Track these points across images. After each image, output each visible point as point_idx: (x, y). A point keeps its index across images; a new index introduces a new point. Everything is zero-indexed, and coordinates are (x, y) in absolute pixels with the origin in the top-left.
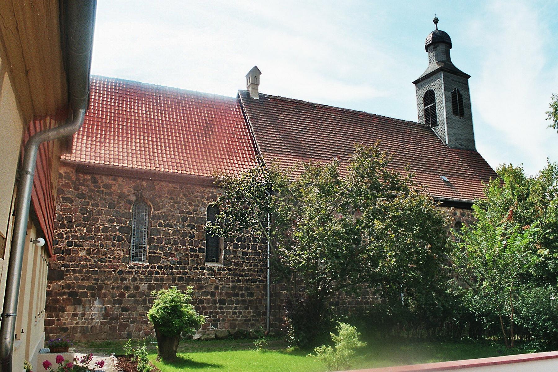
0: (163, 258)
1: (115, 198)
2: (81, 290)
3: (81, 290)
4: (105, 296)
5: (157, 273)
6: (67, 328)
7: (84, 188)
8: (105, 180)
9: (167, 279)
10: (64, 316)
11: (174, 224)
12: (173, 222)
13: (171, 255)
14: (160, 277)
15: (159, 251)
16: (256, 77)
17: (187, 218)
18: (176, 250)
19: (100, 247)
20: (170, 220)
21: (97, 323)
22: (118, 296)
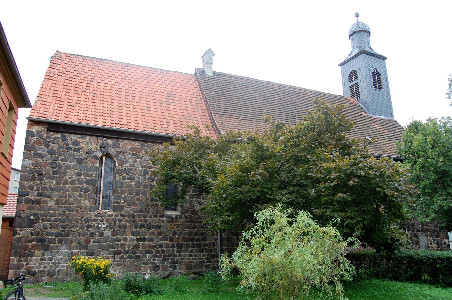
0: (126, 207)
1: (83, 154)
2: (49, 237)
3: (49, 237)
4: (72, 242)
5: (120, 221)
6: (35, 272)
7: (54, 145)
8: (73, 138)
9: (129, 226)
10: (32, 260)
11: (137, 177)
12: (136, 175)
13: (133, 204)
14: (123, 224)
15: (122, 201)
16: (210, 57)
17: (148, 172)
18: (138, 200)
19: (67, 198)
20: (133, 174)
21: (64, 267)
22: (85, 242)
